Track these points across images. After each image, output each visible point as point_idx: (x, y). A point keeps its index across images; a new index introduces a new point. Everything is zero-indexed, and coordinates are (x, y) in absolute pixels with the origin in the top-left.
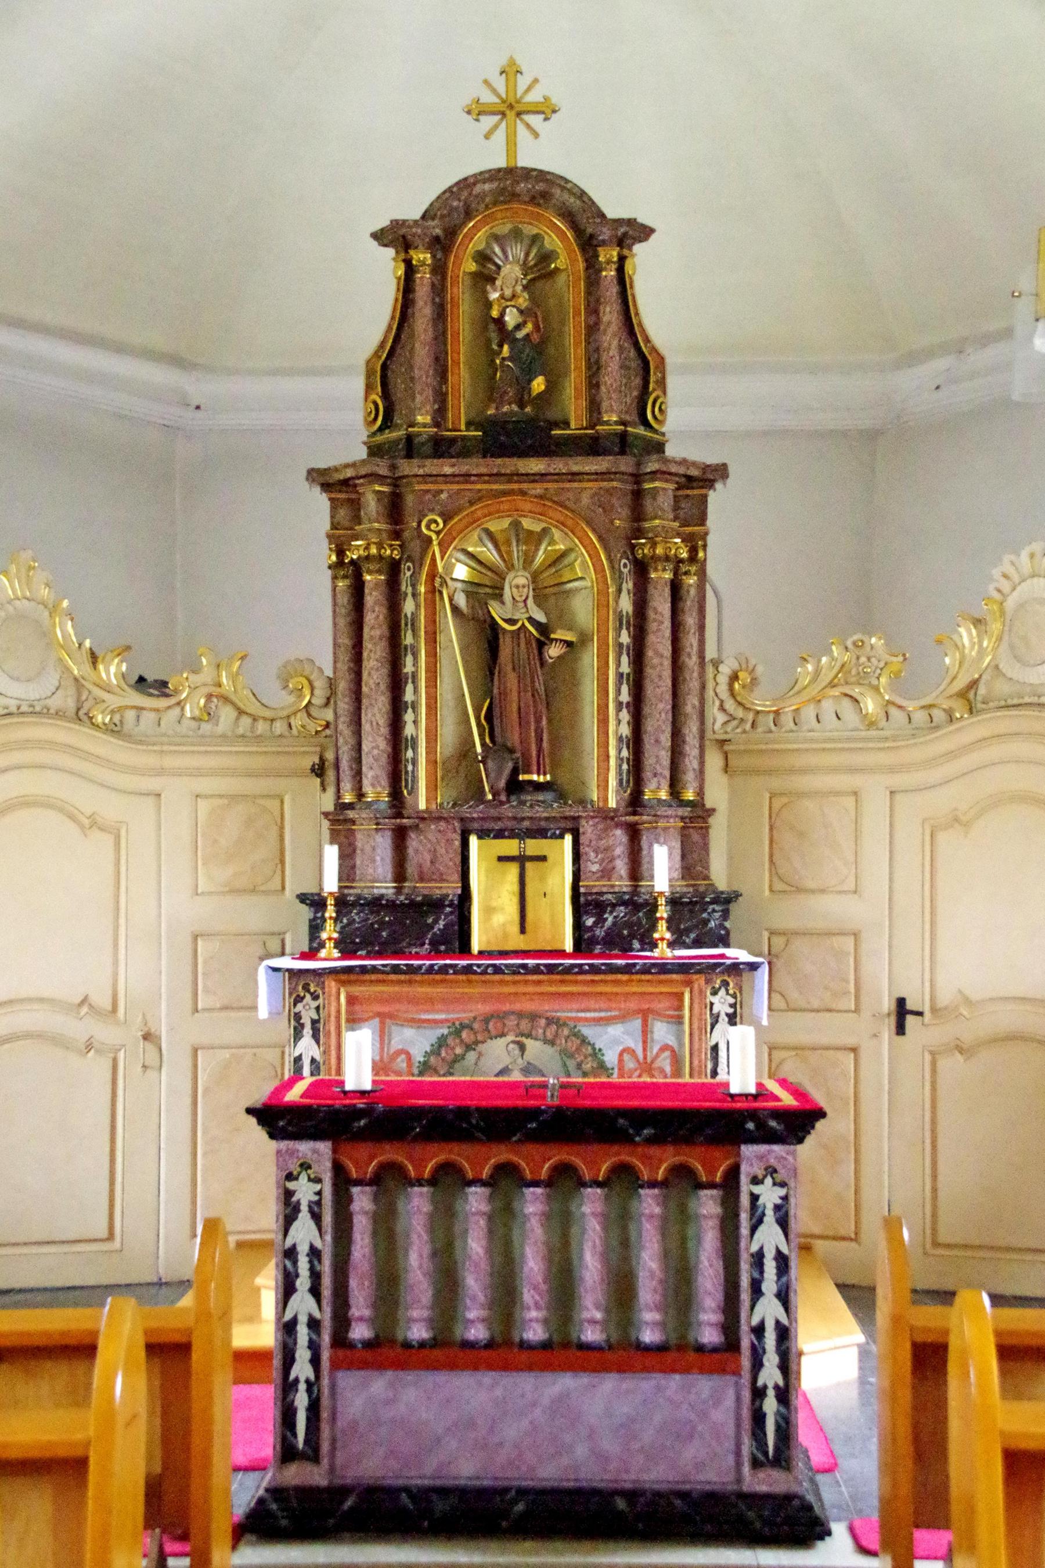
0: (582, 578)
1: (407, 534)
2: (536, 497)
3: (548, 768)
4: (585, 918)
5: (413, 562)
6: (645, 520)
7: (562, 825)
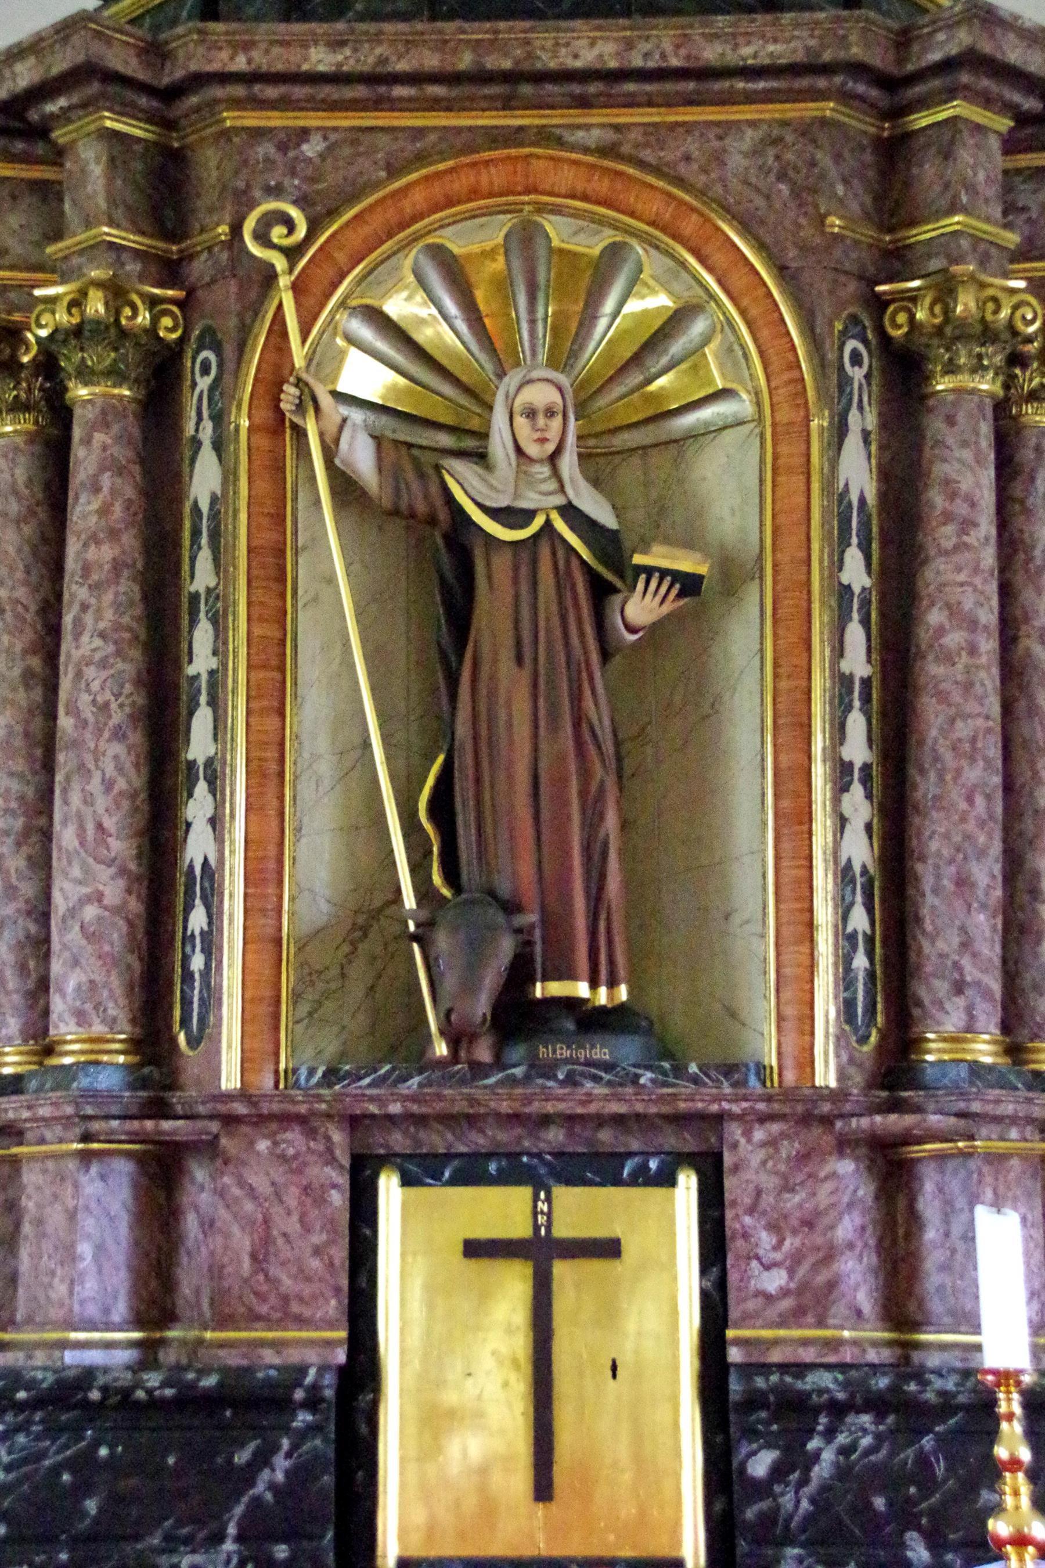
0: (724, 394)
1: (199, 268)
2: (586, 150)
3: (622, 972)
4: (744, 1449)
5: (217, 348)
6: (913, 223)
7: (671, 1140)
